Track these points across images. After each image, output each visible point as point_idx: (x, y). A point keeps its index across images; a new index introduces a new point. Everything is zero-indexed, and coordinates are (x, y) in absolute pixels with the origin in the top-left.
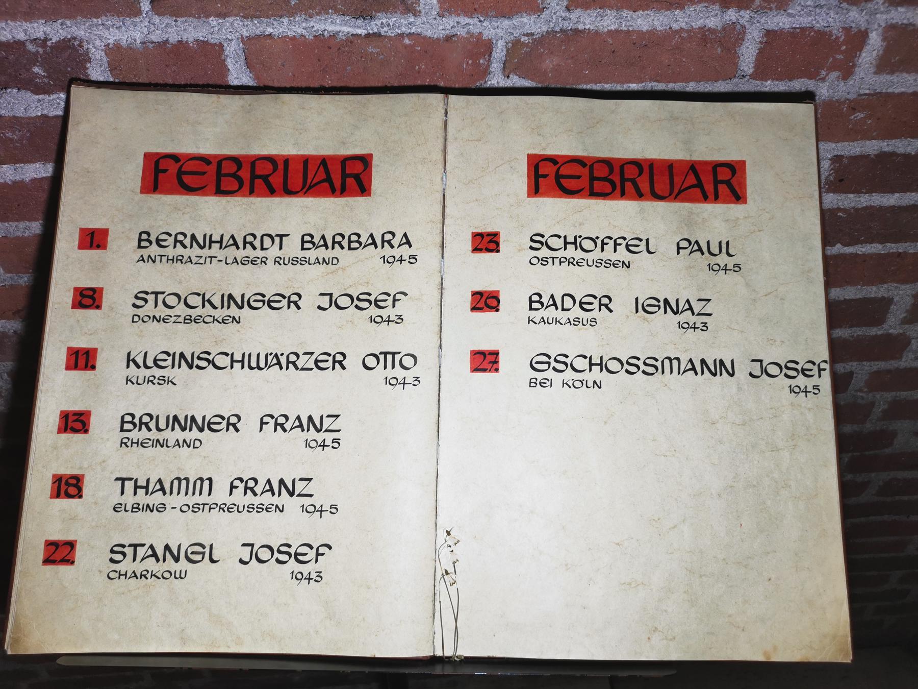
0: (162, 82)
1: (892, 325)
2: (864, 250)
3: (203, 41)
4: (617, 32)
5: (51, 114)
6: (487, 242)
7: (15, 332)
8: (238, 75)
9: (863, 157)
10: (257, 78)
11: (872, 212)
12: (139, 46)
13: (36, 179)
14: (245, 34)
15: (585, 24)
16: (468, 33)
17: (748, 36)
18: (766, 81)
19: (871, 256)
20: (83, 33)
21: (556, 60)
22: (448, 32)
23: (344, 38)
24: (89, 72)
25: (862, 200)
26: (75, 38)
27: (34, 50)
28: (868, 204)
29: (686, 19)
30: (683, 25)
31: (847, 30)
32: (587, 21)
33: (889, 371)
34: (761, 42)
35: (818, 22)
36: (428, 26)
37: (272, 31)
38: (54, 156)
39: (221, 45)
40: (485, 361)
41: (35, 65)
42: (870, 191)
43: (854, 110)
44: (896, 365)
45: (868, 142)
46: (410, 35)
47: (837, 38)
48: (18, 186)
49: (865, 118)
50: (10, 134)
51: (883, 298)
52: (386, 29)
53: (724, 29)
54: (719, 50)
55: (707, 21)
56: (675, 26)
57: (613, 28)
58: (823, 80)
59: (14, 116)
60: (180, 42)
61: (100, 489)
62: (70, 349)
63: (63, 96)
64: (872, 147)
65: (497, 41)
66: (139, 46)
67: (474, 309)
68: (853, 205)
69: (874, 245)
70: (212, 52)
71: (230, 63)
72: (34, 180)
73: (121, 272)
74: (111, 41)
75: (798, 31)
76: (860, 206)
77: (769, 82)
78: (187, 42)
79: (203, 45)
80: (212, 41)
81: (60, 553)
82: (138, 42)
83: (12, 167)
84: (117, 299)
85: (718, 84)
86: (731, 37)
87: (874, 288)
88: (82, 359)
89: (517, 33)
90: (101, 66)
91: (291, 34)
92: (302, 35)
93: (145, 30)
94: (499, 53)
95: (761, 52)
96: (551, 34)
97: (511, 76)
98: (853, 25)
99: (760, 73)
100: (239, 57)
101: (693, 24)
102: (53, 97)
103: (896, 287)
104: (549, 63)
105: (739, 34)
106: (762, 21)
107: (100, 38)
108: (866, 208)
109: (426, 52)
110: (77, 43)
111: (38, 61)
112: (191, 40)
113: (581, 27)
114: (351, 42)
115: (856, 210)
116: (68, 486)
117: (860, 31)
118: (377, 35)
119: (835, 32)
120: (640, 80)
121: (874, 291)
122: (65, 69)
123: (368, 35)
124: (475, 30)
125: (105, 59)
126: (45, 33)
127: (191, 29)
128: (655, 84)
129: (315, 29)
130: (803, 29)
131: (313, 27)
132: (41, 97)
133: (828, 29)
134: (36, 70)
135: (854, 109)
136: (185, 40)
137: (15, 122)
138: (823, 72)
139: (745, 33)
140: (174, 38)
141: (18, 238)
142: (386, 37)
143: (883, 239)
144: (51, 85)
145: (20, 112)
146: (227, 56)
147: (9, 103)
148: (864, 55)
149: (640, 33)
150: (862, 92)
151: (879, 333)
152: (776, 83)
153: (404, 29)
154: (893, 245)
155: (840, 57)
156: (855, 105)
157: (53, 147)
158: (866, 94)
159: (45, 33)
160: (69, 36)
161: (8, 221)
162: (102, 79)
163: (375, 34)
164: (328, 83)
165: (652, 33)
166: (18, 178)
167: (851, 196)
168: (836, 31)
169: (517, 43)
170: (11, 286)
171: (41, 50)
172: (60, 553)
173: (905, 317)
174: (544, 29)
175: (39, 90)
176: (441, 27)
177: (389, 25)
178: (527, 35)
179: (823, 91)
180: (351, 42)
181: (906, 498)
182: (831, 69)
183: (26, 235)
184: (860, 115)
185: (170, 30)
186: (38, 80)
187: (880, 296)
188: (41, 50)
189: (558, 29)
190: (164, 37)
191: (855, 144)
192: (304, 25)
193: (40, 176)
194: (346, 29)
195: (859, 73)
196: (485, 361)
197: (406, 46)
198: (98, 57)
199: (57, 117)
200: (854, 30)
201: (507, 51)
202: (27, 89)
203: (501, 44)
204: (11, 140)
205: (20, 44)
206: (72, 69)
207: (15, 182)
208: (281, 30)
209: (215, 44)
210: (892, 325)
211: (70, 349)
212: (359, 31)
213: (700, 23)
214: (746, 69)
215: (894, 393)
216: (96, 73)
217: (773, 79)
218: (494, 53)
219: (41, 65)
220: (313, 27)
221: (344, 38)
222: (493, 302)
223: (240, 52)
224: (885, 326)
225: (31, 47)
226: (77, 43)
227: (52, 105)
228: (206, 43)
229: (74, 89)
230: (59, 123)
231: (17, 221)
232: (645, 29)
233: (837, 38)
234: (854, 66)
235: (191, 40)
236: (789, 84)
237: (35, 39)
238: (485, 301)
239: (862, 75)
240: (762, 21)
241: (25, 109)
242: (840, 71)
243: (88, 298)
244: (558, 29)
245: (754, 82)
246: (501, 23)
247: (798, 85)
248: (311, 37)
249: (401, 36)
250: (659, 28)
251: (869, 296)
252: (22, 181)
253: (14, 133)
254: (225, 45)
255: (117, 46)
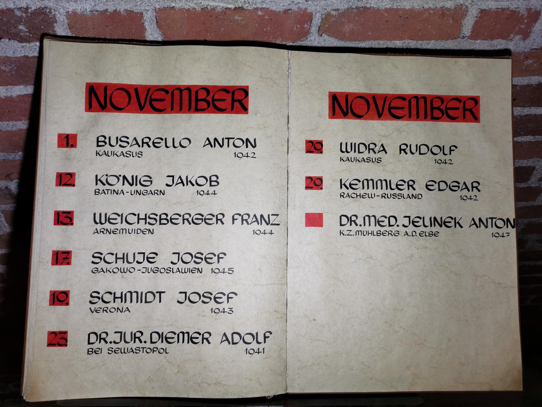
0: (103, 37)
1: (533, 182)
2: (522, 139)
3: (130, 11)
4: (390, 9)
5: (30, 55)
6: (314, 147)
7: (6, 187)
8: (152, 33)
9: (529, 86)
10: (164, 34)
11: (529, 118)
12: (89, 13)
13: (20, 95)
14: (157, 7)
15: (371, 4)
16: (298, 8)
17: (469, 13)
18: (477, 40)
19: (526, 142)
20: (52, 4)
21: (351, 26)
22: (286, 7)
23: (220, 10)
24: (56, 29)
25: (525, 111)
26: (46, 8)
27: (20, 15)
28: (528, 113)
29: (433, 2)
30: (431, 6)
31: (529, 10)
32: (373, 2)
33: (528, 207)
34: (476, 17)
35: (512, 5)
36: (274, 3)
37: (174, 5)
38: (33, 82)
39: (142, 14)
40: (314, 220)
41: (20, 24)
42: (530, 106)
43: (527, 58)
44: (532, 204)
45: (533, 77)
46: (262, 9)
47: (523, 15)
48: (9, 99)
49: (533, 63)
50: (4, 67)
51: (530, 167)
52: (247, 5)
53: (456, 8)
54: (451, 21)
55: (446, 4)
56: (426, 6)
57: (388, 7)
58: (511, 40)
59: (6, 56)
60: (115, 11)
61: (79, 299)
62: (55, 212)
63: (38, 44)
64: (534, 80)
65: (316, 13)
66: (89, 13)
67: (307, 188)
68: (519, 113)
69: (529, 137)
70: (136, 18)
71: (147, 25)
72: (19, 96)
73: (86, 163)
74: (70, 10)
75: (500, 10)
76: (523, 114)
77: (479, 41)
78: (120, 11)
79: (130, 13)
80: (136, 11)
81: (58, 339)
82: (88, 10)
83: (5, 88)
84: (85, 180)
85: (448, 42)
86: (459, 13)
87: (526, 161)
88: (64, 218)
89: (329, 9)
90: (63, 26)
91: (187, 7)
92: (194, 8)
93: (93, 4)
94: (317, 21)
95: (476, 22)
96: (350, 9)
97: (323, 35)
98: (533, 7)
99: (475, 35)
100: (153, 21)
101: (437, 5)
102: (32, 44)
103: (538, 161)
104: (347, 28)
105: (464, 12)
106: (479, 4)
107: (63, 8)
108: (526, 116)
109: (271, 20)
110: (48, 11)
111: (22, 22)
112: (122, 10)
113: (368, 6)
114: (225, 13)
115: (521, 116)
116: (59, 298)
117: (536, 11)
118: (241, 9)
119: (522, 11)
120: (401, 39)
121: (524, 163)
122: (41, 28)
123: (236, 9)
124: (303, 7)
125: (66, 21)
126: (27, 4)
127: (122, 3)
128: (411, 41)
129: (202, 4)
130: (503, 9)
131: (201, 3)
132: (24, 44)
133: (517, 10)
134: (21, 27)
135: (527, 58)
136: (118, 10)
137: (7, 60)
138: (512, 36)
139: (467, 11)
140: (111, 9)
141: (8, 132)
142: (246, 10)
143: (533, 133)
144: (31, 37)
145: (10, 54)
146: (145, 20)
147: (3, 48)
148: (537, 25)
149: (404, 10)
150: (533, 47)
151: (525, 186)
152: (483, 41)
153: (258, 5)
154: (539, 137)
155: (523, 26)
156: (527, 56)
157: (32, 75)
158: (535, 49)
159: (27, 4)
160: (43, 6)
161: (2, 121)
162: (63, 34)
163: (239, 7)
164: (209, 38)
165: (412, 10)
166: (9, 95)
167: (519, 108)
168: (523, 12)
169: (328, 15)
170: (4, 160)
171: (24, 15)
172: (58, 339)
173: (541, 178)
174: (346, 7)
175: (22, 40)
176: (282, 5)
177: (249, 3)
178: (335, 10)
179: (511, 46)
180: (225, 13)
181: (528, 276)
182: (517, 33)
183: (14, 129)
184: (530, 61)
185: (109, 3)
186: (22, 34)
187: (528, 165)
188: (24, 15)
189: (354, 7)
190: (105, 8)
191: (525, 78)
192: (195, 1)
193: (23, 94)
194: (222, 4)
195: (533, 36)
196: (314, 220)
197: (259, 16)
198: (62, 20)
199: (34, 57)
200: (533, 11)
201: (322, 19)
202: (15, 40)
203: (318, 15)
204: (4, 71)
205: (10, 11)
206: (45, 27)
207: (6, 97)
208: (180, 5)
209: (138, 13)
210: (533, 182)
211: (55, 212)
212: (230, 6)
213: (441, 4)
214: (466, 33)
215: (529, 219)
216: (61, 31)
217: (481, 39)
218: (313, 21)
219: (25, 25)
220: (201, 3)
221: (220, 10)
222: (318, 182)
223: (154, 19)
224: (529, 182)
225: (18, 13)
226: (48, 11)
227: (31, 50)
228: (132, 12)
229: (46, 42)
230: (36, 60)
231: (8, 121)
232: (407, 8)
233: (523, 15)
234: (530, 32)
235: (122, 10)
236: (490, 42)
237: (20, 8)
238: (314, 183)
239: (535, 37)
240: (479, 4)
241: (14, 52)
242: (521, 34)
243: (65, 180)
244: (354, 7)
245: (470, 41)
246: (320, 2)
247: (499, 44)
248: (200, 9)
249: (257, 9)
250: (417, 7)
251: (522, 165)
252: (11, 97)
253: (6, 66)
254: (144, 13)
255: (75, 13)
